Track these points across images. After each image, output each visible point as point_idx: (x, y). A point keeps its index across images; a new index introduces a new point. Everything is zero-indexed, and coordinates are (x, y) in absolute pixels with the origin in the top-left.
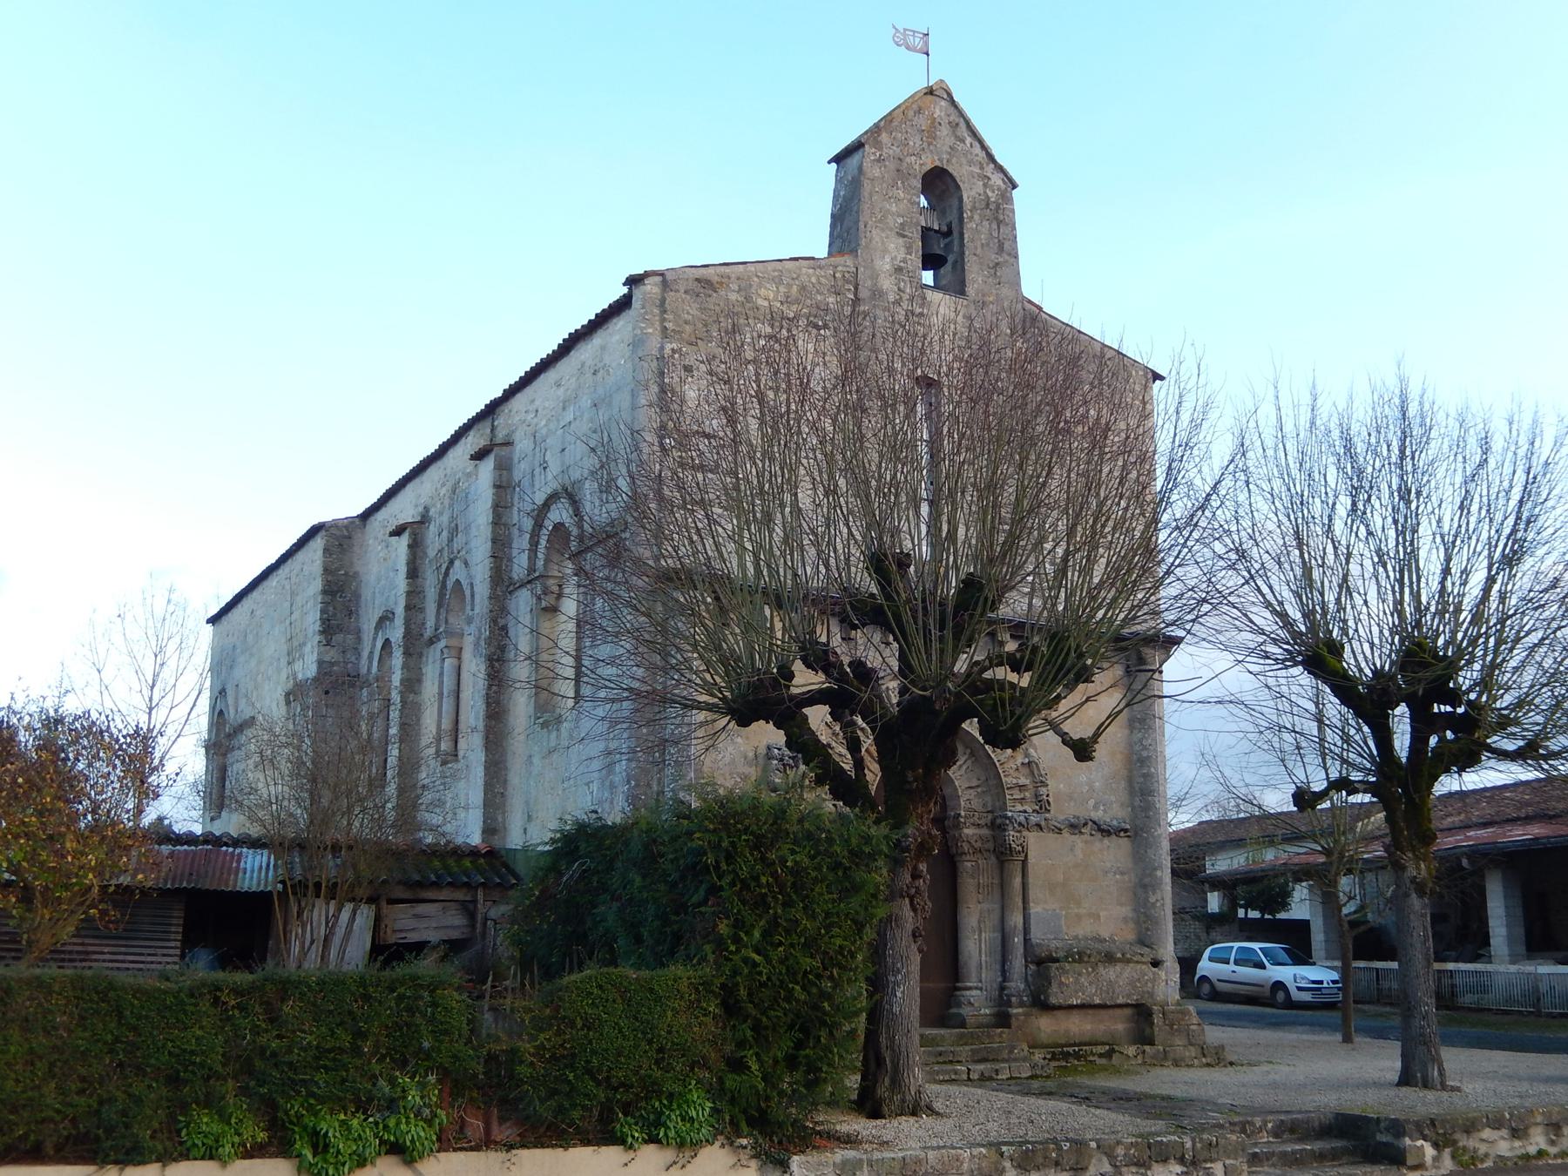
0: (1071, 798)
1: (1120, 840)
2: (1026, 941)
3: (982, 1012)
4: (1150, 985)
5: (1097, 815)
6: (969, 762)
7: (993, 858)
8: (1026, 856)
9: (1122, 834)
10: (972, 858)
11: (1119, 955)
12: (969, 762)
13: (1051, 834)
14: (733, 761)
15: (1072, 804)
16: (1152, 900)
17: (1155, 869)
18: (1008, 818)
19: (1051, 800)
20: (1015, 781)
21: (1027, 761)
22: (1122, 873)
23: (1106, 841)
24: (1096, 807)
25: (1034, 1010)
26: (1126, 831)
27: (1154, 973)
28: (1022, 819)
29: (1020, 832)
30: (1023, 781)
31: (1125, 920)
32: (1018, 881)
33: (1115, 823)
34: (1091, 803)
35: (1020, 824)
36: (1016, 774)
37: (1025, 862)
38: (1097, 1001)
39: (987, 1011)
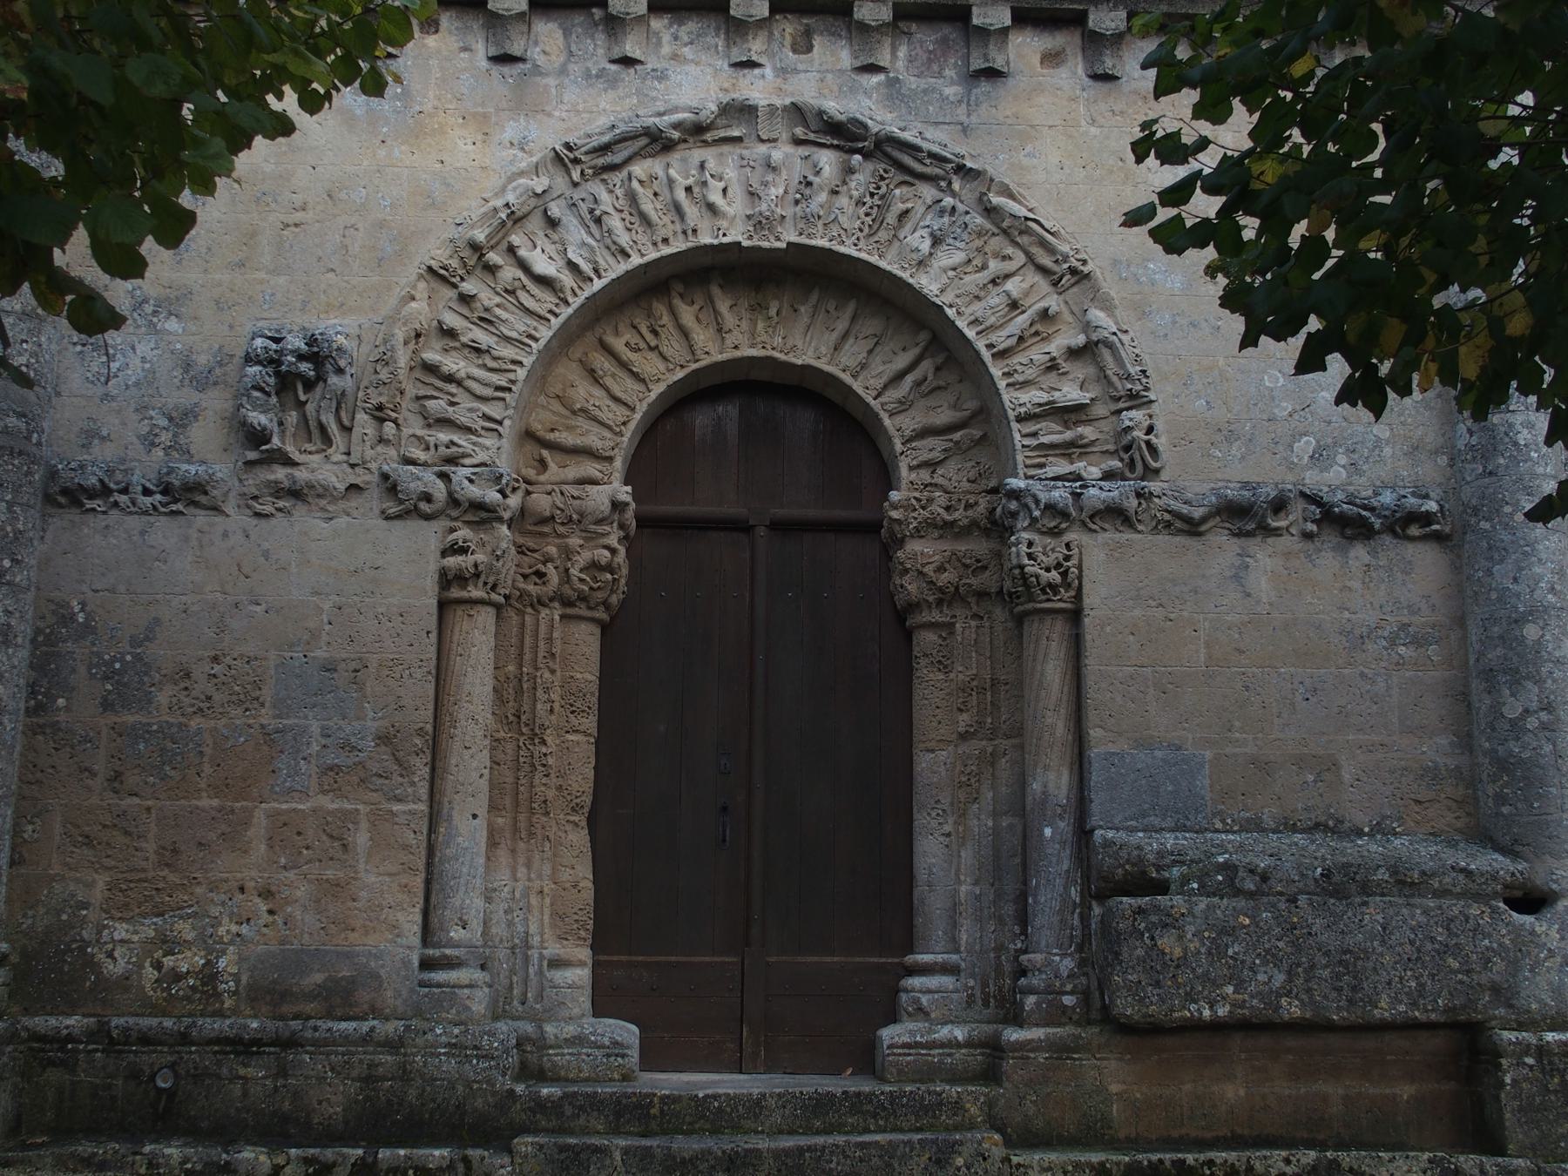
0: (1231, 437)
1: (1412, 551)
2: (1083, 833)
3: (944, 1032)
4: (1499, 965)
5: (1331, 480)
6: (926, 366)
7: (999, 613)
8: (1079, 596)
9: (1414, 531)
10: (936, 616)
11: (1382, 875)
12: (926, 366)
13: (1163, 539)
14: (150, 377)
15: (1236, 450)
16: (1512, 709)
17: (1520, 621)
18: (1015, 494)
19: (1160, 442)
20: (1043, 397)
21: (1081, 340)
22: (1418, 642)
23: (1359, 553)
24: (1320, 457)
25: (1090, 1033)
26: (1426, 519)
27: (1517, 931)
28: (1060, 494)
29: (1055, 533)
30: (1070, 393)
31: (1431, 774)
32: (1052, 671)
33: (1387, 498)
34: (1306, 445)
35: (1051, 508)
36: (1051, 379)
37: (1075, 616)
38: (1292, 1009)
39: (960, 1034)
